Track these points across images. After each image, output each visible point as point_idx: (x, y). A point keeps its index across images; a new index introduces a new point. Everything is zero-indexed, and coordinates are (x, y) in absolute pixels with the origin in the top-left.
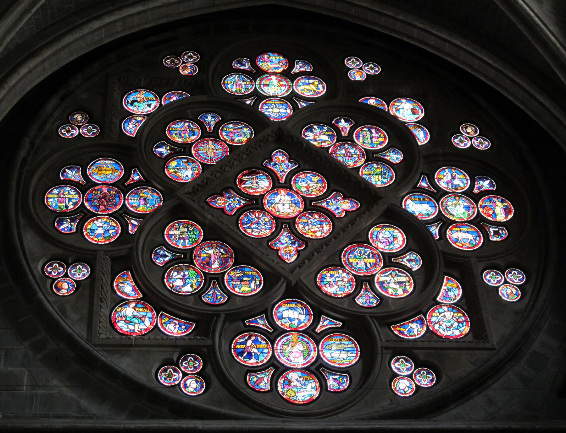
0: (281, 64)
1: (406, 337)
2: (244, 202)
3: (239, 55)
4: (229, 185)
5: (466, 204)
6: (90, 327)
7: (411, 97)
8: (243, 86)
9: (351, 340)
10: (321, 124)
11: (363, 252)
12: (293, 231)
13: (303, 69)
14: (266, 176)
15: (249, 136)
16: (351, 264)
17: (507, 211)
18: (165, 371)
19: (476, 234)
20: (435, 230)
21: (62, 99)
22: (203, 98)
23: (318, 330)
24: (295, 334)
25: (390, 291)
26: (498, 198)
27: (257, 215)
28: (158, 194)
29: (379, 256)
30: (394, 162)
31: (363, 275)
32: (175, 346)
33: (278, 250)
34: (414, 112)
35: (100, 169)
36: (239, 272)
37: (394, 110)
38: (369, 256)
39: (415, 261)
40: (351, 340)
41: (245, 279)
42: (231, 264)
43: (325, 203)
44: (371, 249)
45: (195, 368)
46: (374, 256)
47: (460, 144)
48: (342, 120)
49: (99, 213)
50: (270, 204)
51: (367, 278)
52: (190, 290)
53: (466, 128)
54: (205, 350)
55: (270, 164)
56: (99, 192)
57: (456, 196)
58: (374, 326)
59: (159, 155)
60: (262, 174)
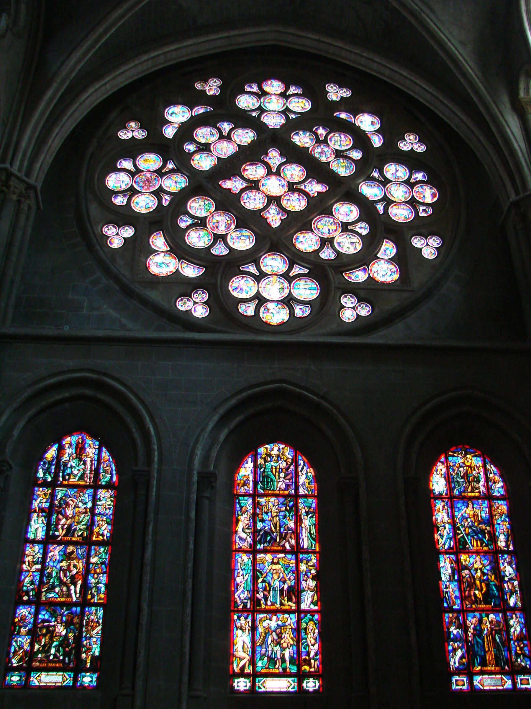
0: (280, 88)
1: (353, 281)
2: (246, 185)
3: (250, 81)
4: (236, 173)
7: (371, 112)
8: (251, 103)
9: (314, 282)
10: (305, 130)
11: (327, 221)
13: (296, 92)
14: (263, 166)
15: (253, 139)
16: (318, 229)
17: (433, 195)
18: (182, 300)
19: (409, 211)
20: (380, 207)
23: (291, 274)
24: (276, 276)
26: (428, 186)
27: (254, 194)
28: (185, 178)
29: (339, 224)
30: (356, 159)
31: (326, 237)
33: (267, 218)
34: (373, 123)
35: (145, 161)
36: (238, 233)
37: (359, 122)
38: (331, 224)
39: (365, 228)
40: (314, 282)
41: (242, 238)
42: (233, 226)
43: (304, 186)
44: (334, 219)
45: (203, 298)
46: (335, 223)
47: (404, 147)
48: (321, 128)
49: (143, 191)
50: (264, 187)
51: (329, 240)
52: (203, 245)
53: (409, 136)
55: (266, 158)
56: (144, 177)
57: (397, 184)
58: (331, 273)
59: (187, 151)
60: (259, 165)
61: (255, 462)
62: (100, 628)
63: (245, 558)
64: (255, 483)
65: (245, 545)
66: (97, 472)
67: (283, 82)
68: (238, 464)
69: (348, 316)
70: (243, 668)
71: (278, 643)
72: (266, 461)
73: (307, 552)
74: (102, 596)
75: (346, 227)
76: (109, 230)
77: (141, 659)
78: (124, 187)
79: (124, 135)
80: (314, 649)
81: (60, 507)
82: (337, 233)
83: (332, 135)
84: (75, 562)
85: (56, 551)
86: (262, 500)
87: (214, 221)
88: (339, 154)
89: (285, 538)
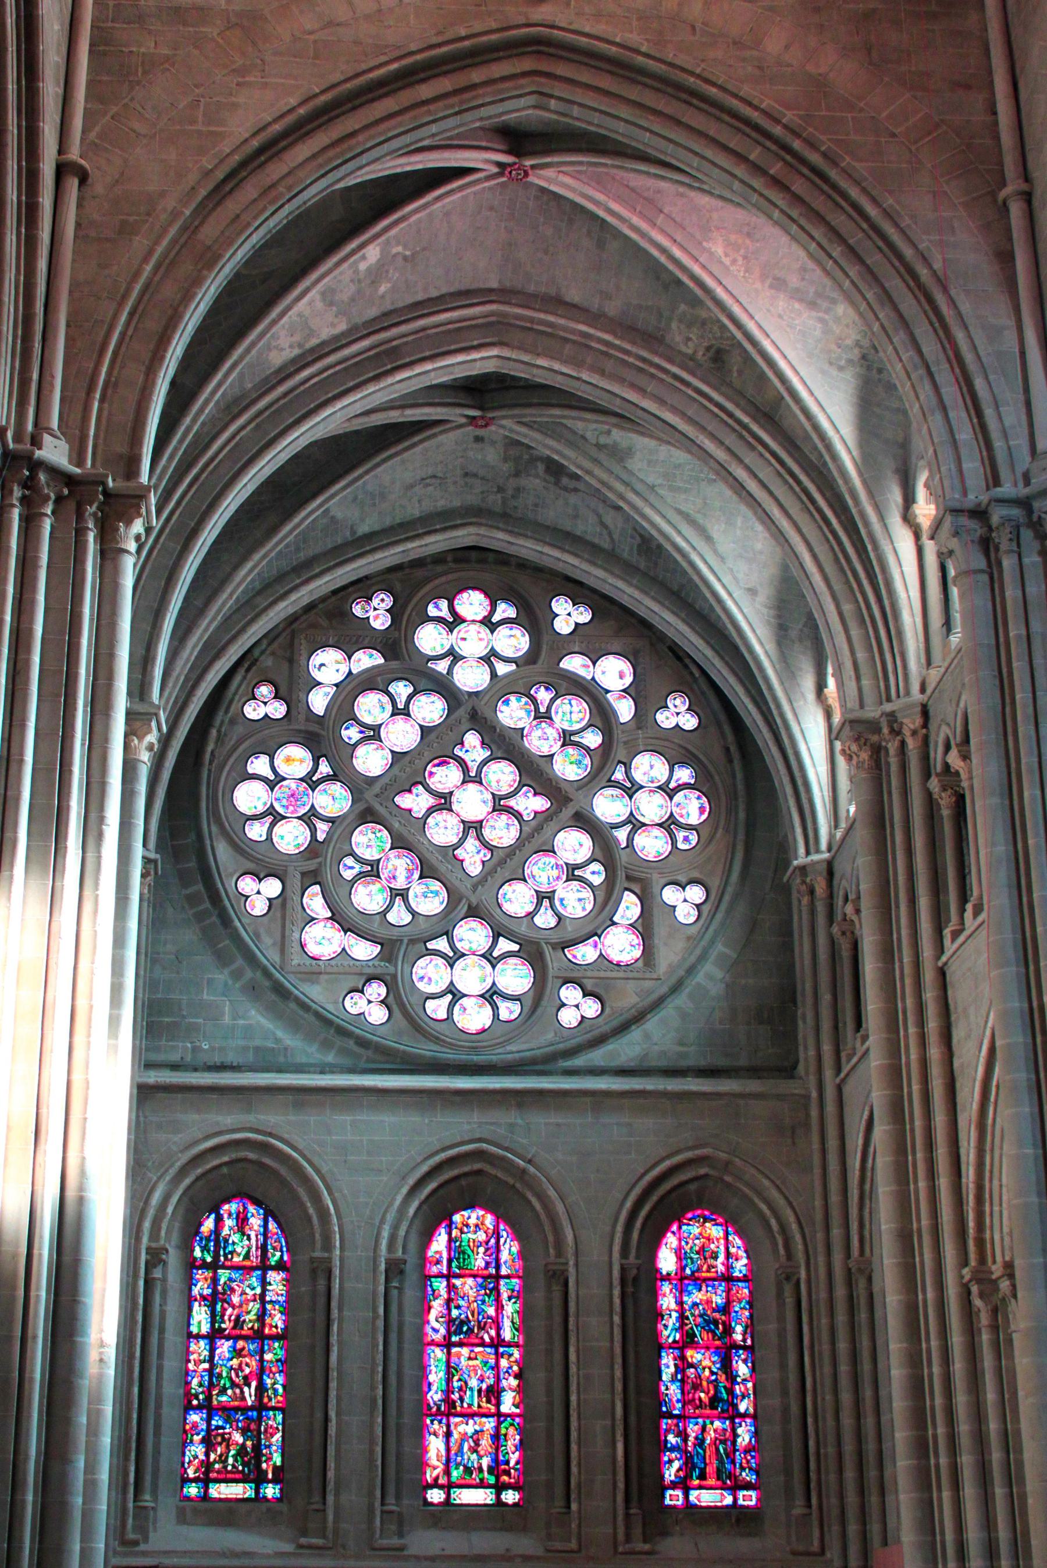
5: (662, 801)
6: (282, 952)
12: (480, 837)
13: (505, 615)
17: (702, 810)
20: (622, 835)
21: (248, 670)
22: (394, 664)
23: (495, 954)
25: (570, 909)
32: (361, 974)
34: (622, 676)
35: (288, 759)
42: (416, 875)
54: (388, 978)
58: (547, 951)
61: (449, 1234)
62: (279, 1435)
63: (439, 1354)
64: (450, 1261)
65: (438, 1337)
66: (263, 1248)
67: (487, 595)
69: (568, 1018)
70: (437, 1478)
71: (474, 1450)
72: (462, 1232)
73: (509, 1345)
74: (280, 1398)
75: (572, 872)
76: (247, 885)
77: (331, 1474)
78: (261, 809)
79: (253, 711)
80: (514, 1458)
81: (224, 1293)
82: (561, 882)
83: (558, 701)
84: (247, 1360)
85: (224, 1347)
86: (457, 1282)
87: (390, 867)
89: (483, 1329)
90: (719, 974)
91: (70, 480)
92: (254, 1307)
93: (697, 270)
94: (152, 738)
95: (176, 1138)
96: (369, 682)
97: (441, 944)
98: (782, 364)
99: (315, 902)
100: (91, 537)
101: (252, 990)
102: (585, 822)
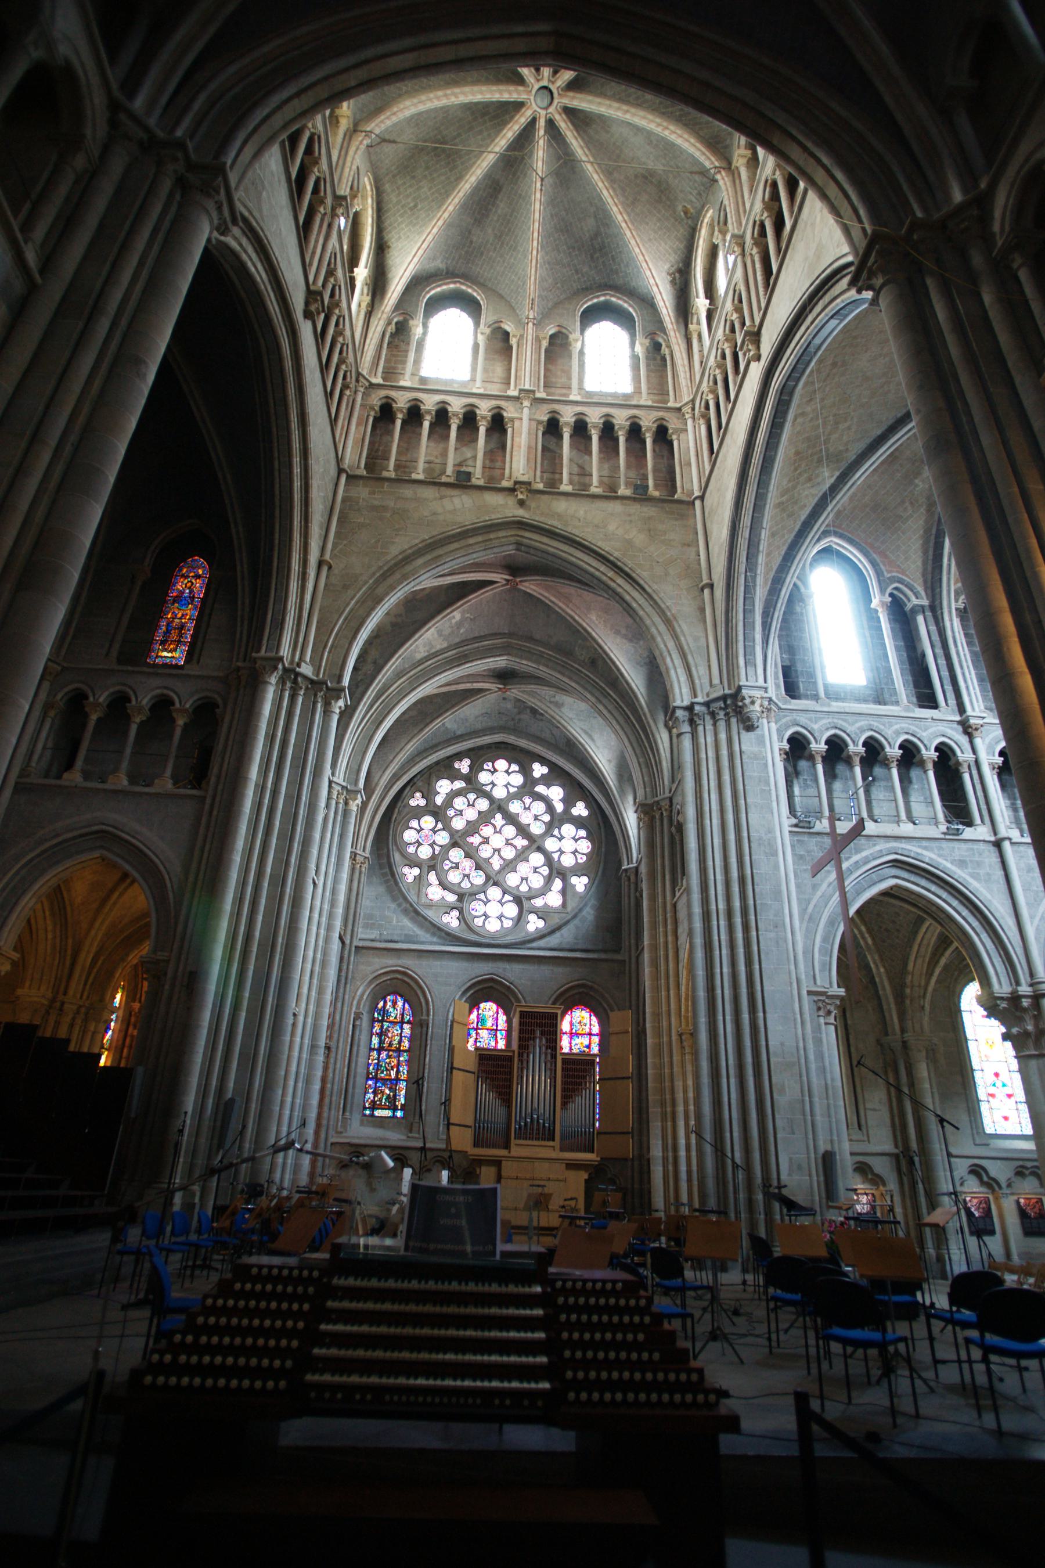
6: (418, 896)
12: (499, 855)
20: (556, 856)
58: (524, 900)
66: (403, 1015)
68: (471, 1012)
75: (535, 870)
76: (406, 870)
79: (413, 803)
85: (384, 1055)
88: (536, 818)
90: (592, 912)
91: (312, 682)
92: (397, 1038)
93: (584, 625)
94: (359, 801)
95: (369, 968)
96: (459, 793)
97: (482, 896)
98: (618, 663)
99: (432, 877)
100: (319, 705)
101: (405, 912)
102: (540, 849)
